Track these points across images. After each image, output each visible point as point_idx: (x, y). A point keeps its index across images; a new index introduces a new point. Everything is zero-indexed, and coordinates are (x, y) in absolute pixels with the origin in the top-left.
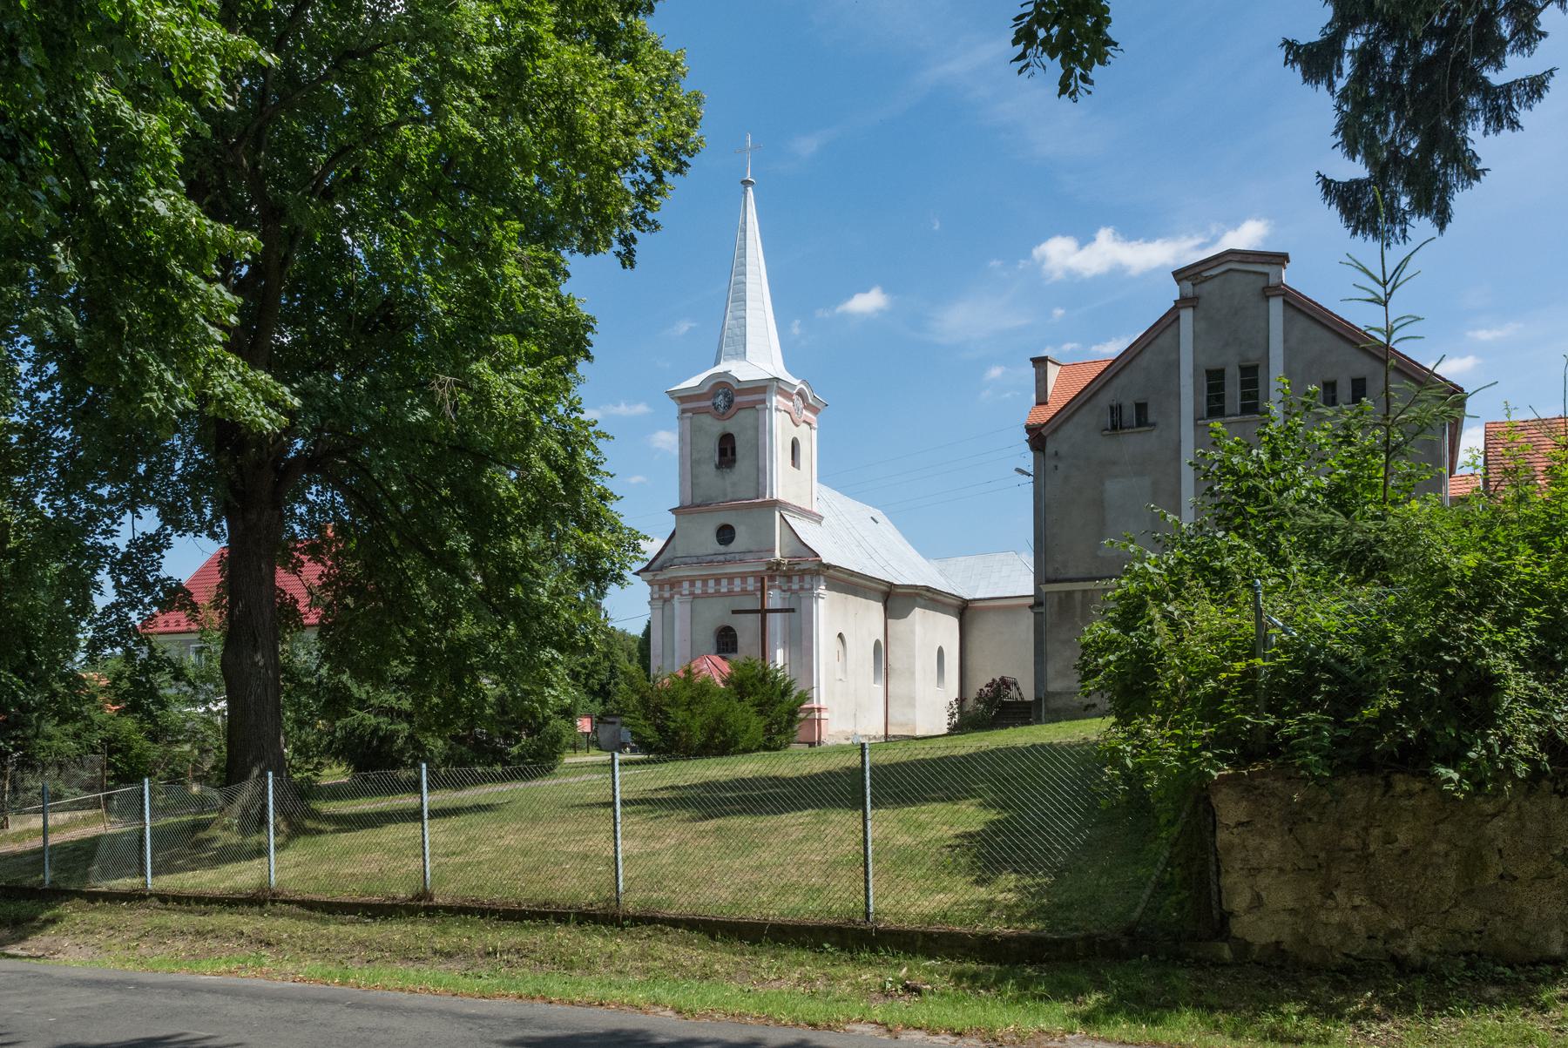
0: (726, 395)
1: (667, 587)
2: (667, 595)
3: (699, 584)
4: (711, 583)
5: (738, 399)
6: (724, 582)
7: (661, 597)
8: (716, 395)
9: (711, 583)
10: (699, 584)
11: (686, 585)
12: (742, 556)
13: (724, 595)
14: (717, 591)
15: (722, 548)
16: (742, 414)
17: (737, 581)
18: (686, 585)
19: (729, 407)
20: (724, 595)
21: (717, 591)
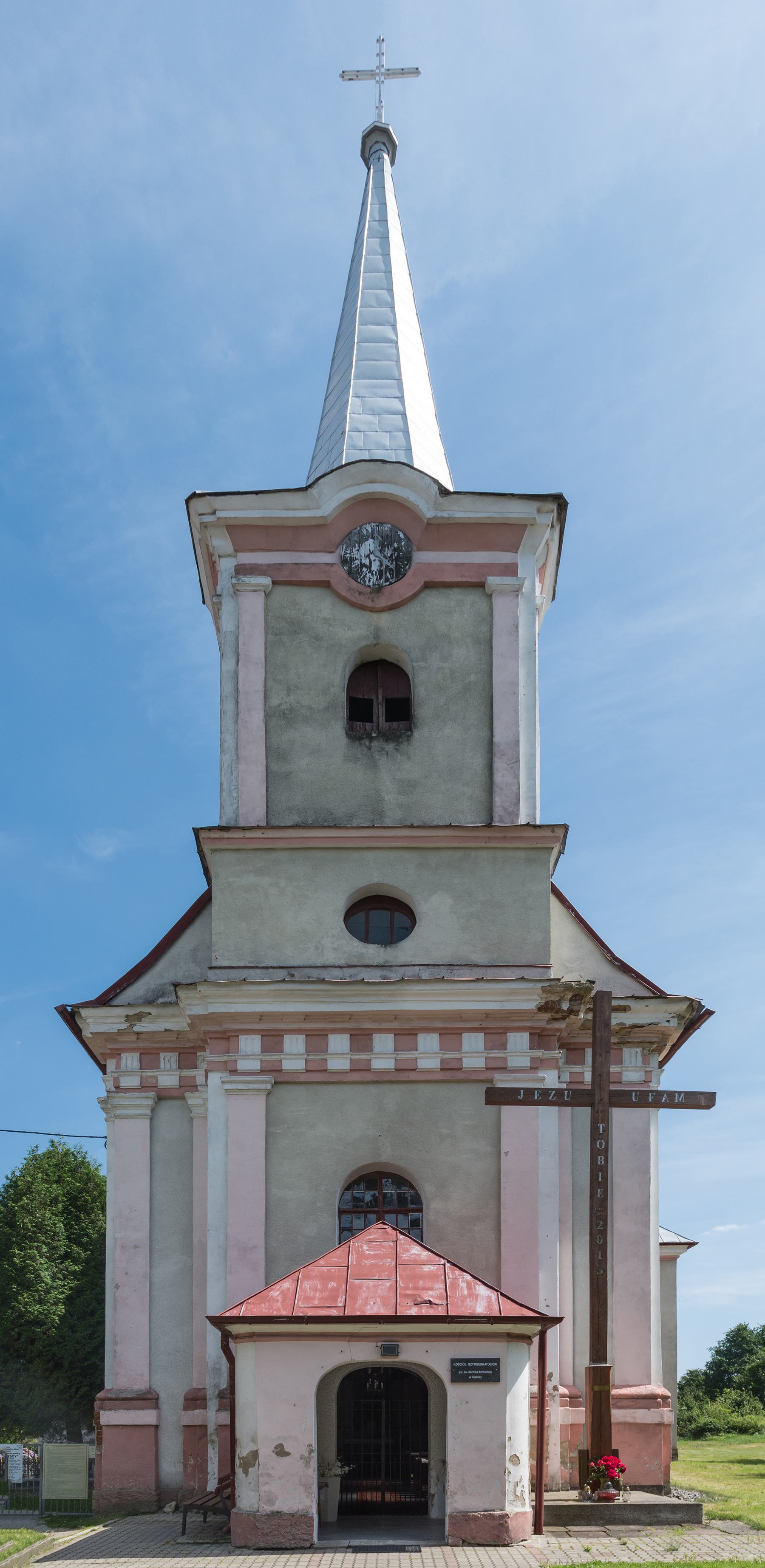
0: (385, 542)
1: (168, 1060)
2: (168, 1079)
3: (294, 1044)
4: (339, 1043)
5: (421, 557)
6: (384, 1043)
7: (143, 1087)
8: (355, 538)
9: (339, 1043)
10: (294, 1044)
11: (250, 1044)
12: (442, 972)
13: (382, 1079)
14: (360, 1068)
15: (373, 952)
16: (434, 601)
17: (429, 1043)
18: (250, 1044)
19: (399, 573)
20: (382, 1079)
21: (360, 1068)
